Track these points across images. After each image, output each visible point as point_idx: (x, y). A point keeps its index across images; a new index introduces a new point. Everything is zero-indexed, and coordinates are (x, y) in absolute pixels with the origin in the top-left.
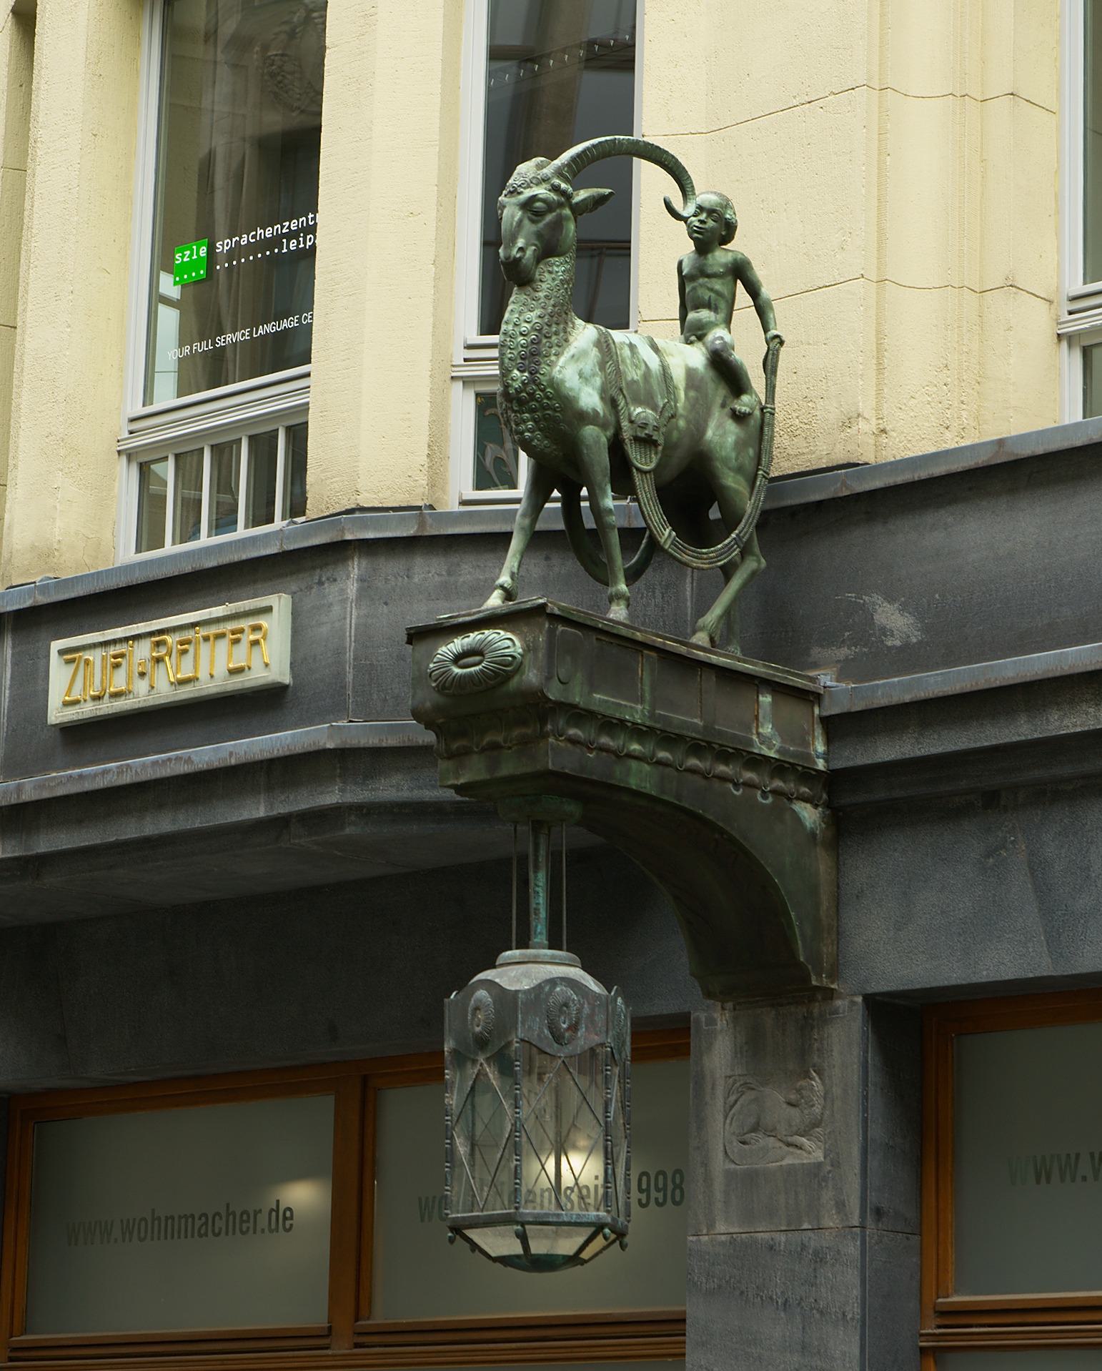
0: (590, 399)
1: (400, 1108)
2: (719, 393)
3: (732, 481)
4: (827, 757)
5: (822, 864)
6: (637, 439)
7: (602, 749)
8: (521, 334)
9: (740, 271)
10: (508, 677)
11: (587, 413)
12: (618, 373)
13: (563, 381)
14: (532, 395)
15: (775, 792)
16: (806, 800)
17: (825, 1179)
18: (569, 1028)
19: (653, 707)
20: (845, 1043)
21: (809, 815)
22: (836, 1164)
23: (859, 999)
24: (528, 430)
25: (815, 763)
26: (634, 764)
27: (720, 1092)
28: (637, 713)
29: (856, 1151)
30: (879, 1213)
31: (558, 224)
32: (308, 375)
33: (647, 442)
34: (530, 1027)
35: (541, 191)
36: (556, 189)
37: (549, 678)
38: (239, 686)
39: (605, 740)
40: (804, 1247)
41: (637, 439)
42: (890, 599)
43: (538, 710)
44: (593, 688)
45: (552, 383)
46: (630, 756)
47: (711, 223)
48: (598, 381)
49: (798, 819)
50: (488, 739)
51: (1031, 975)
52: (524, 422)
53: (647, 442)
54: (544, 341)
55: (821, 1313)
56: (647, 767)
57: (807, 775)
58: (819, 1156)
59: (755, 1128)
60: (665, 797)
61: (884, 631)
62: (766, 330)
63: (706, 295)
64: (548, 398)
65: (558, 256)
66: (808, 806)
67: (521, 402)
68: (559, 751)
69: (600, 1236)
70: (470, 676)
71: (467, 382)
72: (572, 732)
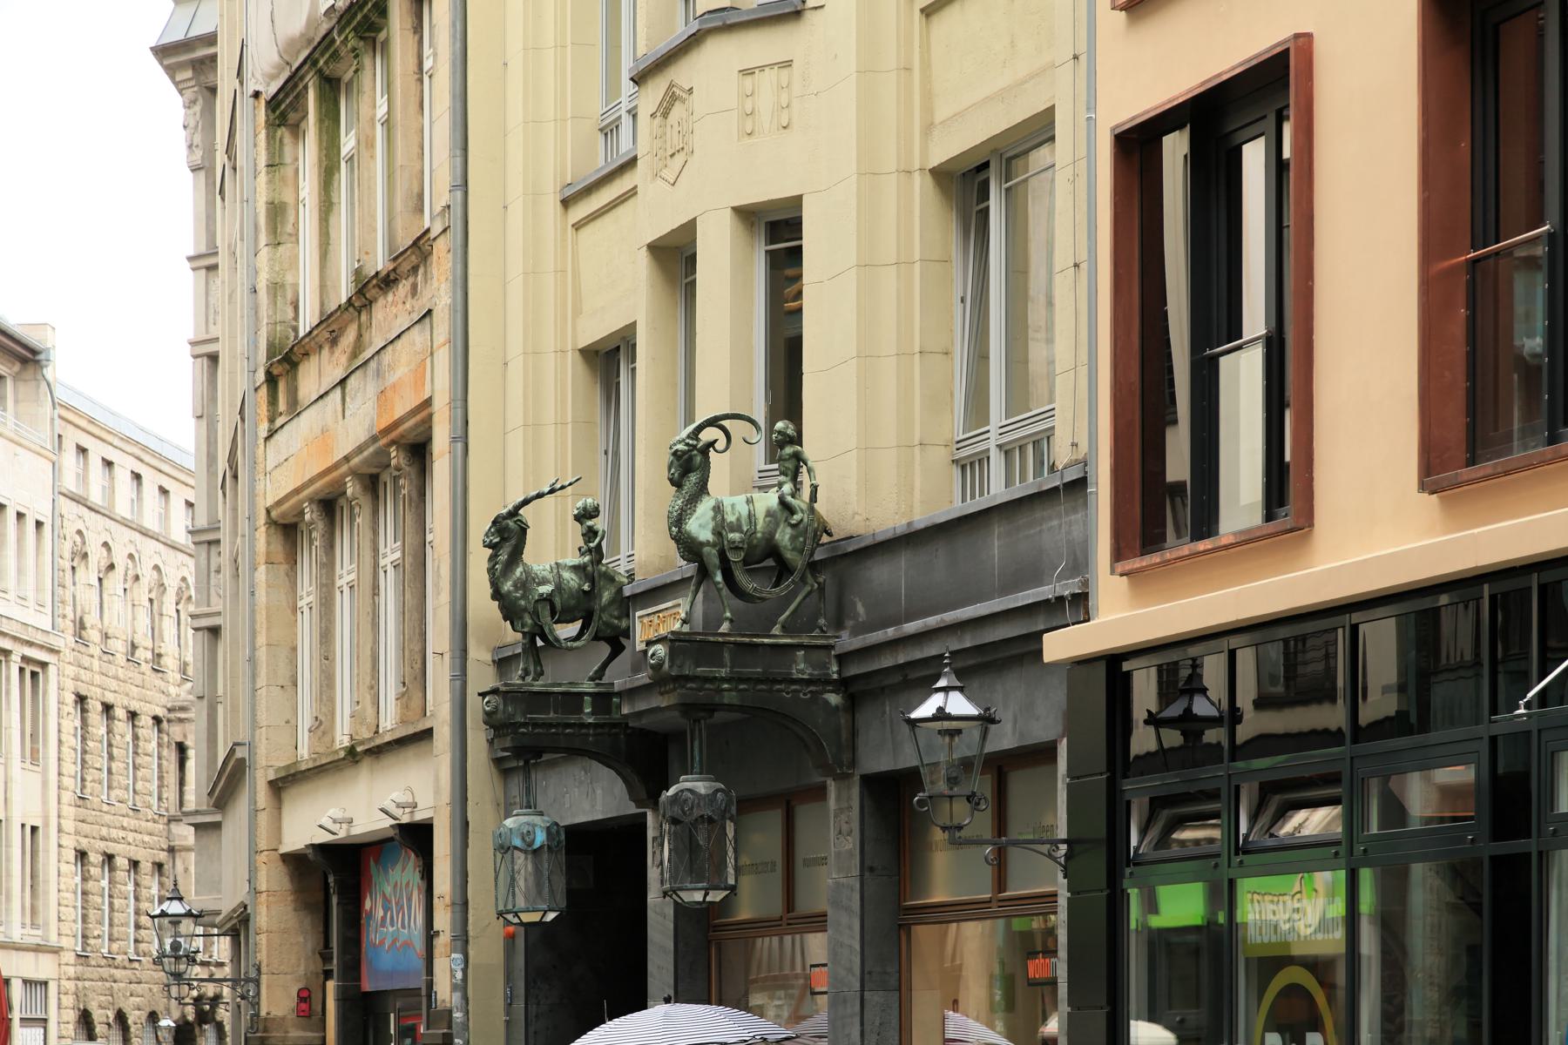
1: (805, 815)
3: (789, 555)
4: (839, 672)
5: (844, 720)
12: (723, 519)
21: (834, 699)
28: (723, 672)
30: (871, 869)
31: (691, 459)
35: (680, 447)
48: (711, 525)
49: (827, 702)
53: (737, 548)
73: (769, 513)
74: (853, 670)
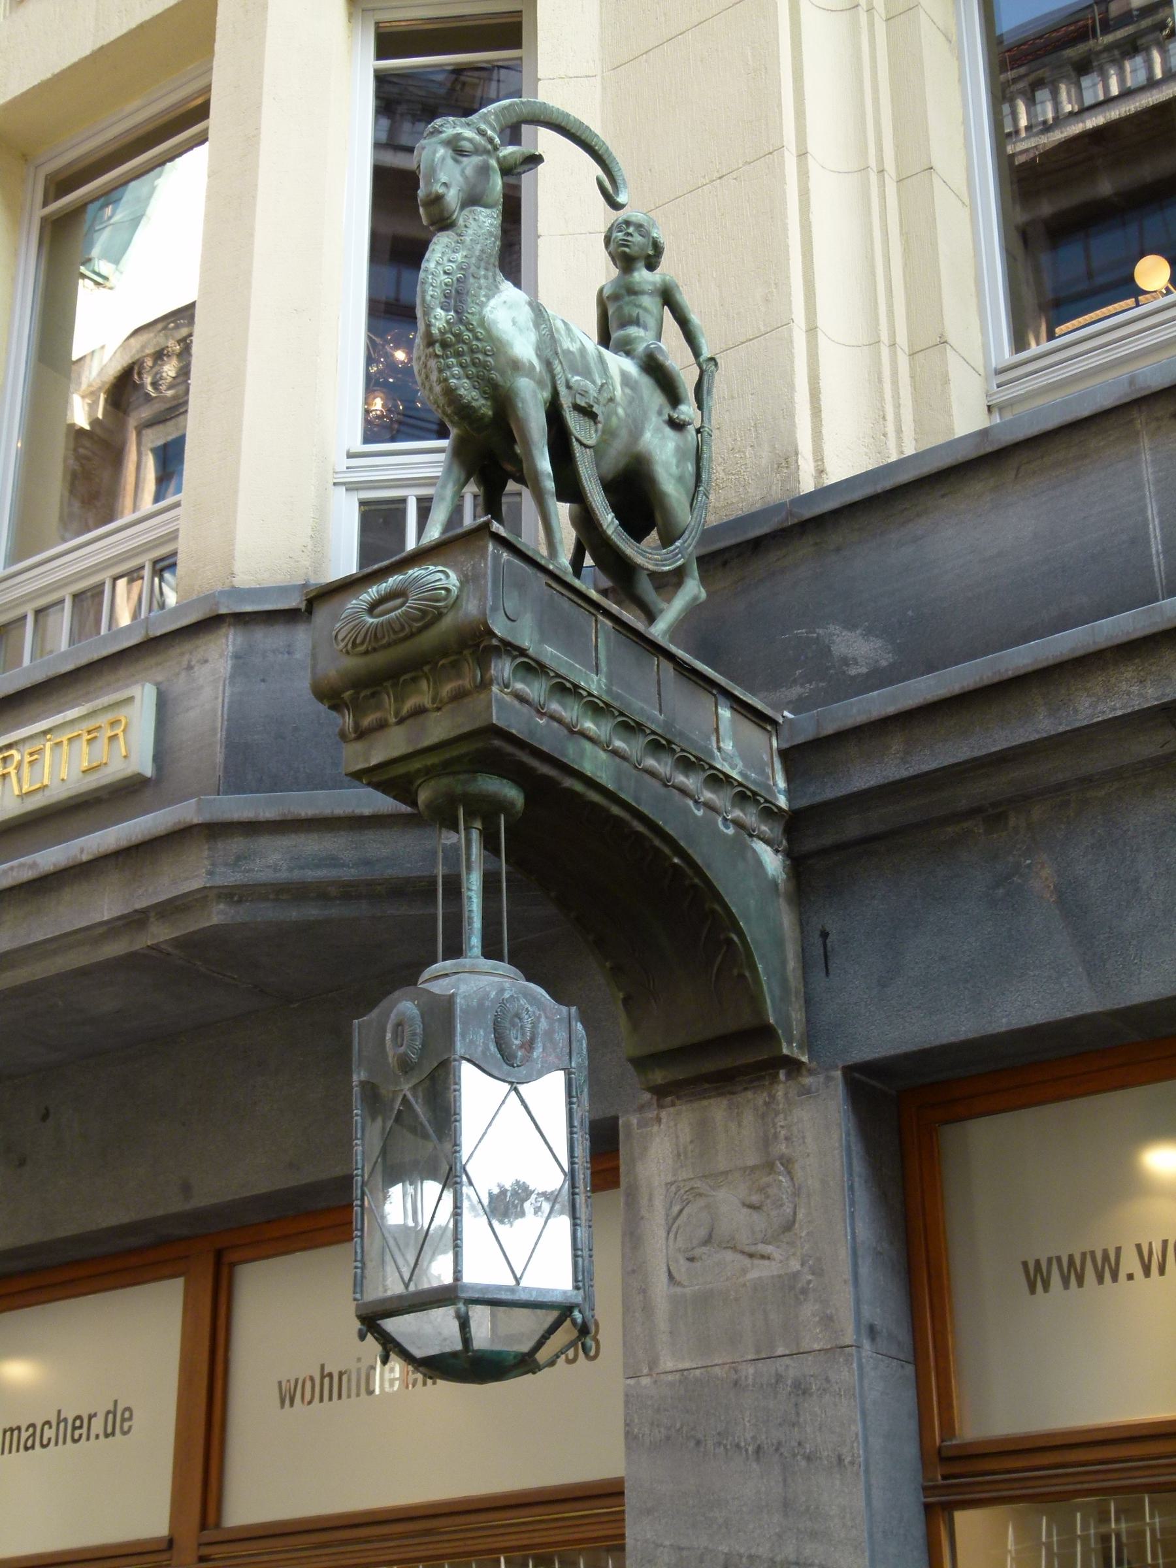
0: (523, 346)
2: (654, 399)
4: (790, 793)
5: (787, 920)
6: (577, 408)
7: (553, 717)
8: (445, 273)
9: (668, 297)
10: (440, 615)
11: (523, 364)
13: (495, 323)
14: (458, 336)
15: (737, 823)
16: (767, 842)
17: (804, 1291)
18: (522, 1047)
19: (610, 677)
20: (816, 1130)
21: (772, 862)
22: (818, 1272)
23: (838, 1074)
24: (453, 376)
25: (777, 799)
26: (588, 746)
27: (659, 1203)
28: (594, 684)
29: (844, 1254)
30: (872, 1332)
32: (177, 505)
33: (587, 413)
34: (471, 1042)
36: (482, 133)
37: (494, 609)
38: (94, 785)
39: (555, 707)
40: (779, 1378)
41: (577, 408)
42: (850, 625)
43: (479, 644)
44: (544, 639)
45: (482, 322)
46: (584, 735)
47: (637, 238)
49: (759, 864)
50: (409, 705)
51: (1069, 1015)
52: (449, 367)
54: (472, 280)
55: (808, 1458)
56: (603, 755)
57: (769, 812)
58: (795, 1265)
59: (707, 1241)
60: (623, 796)
61: (845, 661)
62: (697, 353)
63: (635, 312)
64: (478, 339)
65: (486, 206)
66: (769, 849)
67: (445, 345)
68: (510, 699)
69: (568, 1322)
70: (389, 622)
71: (351, 487)
72: (519, 686)
73: (626, 379)
74: (864, 774)
